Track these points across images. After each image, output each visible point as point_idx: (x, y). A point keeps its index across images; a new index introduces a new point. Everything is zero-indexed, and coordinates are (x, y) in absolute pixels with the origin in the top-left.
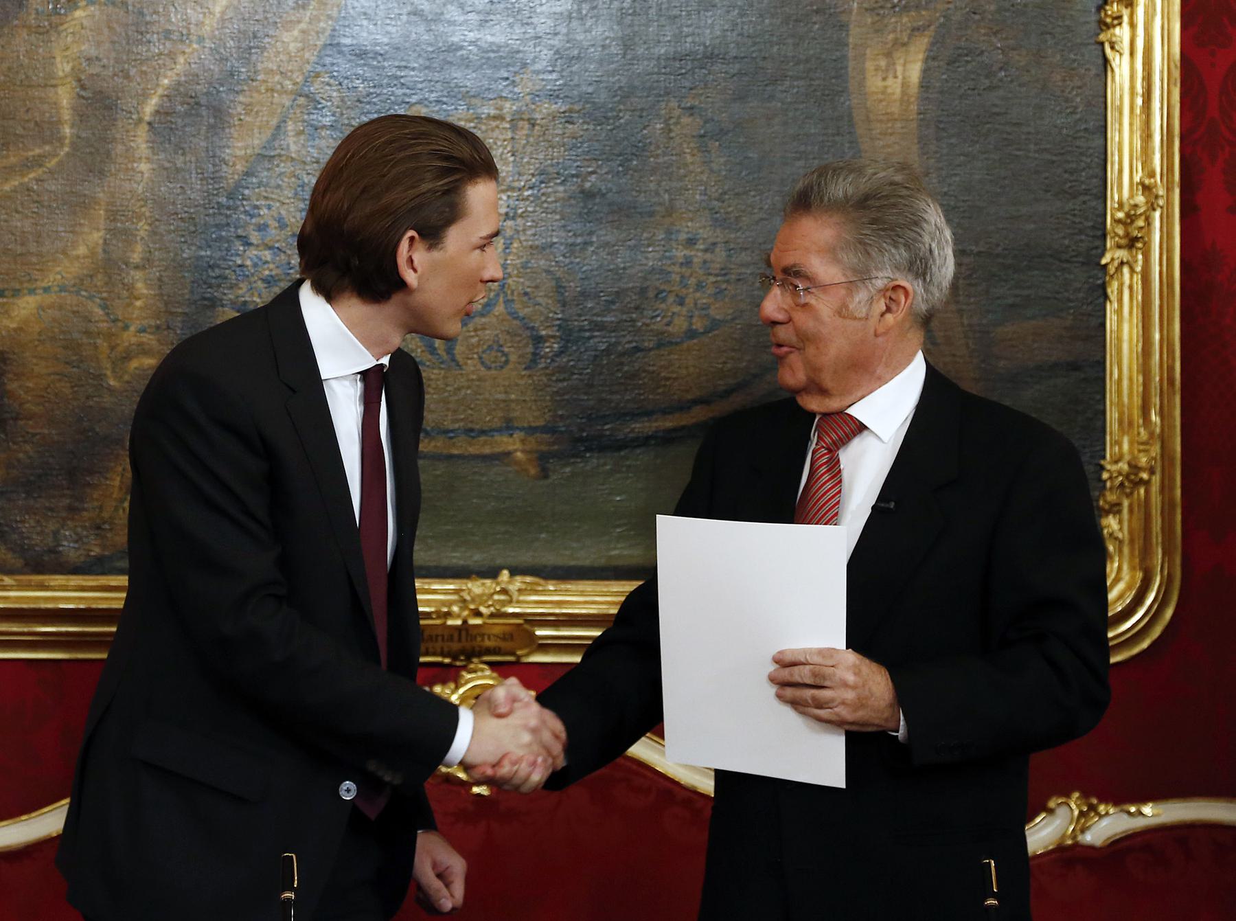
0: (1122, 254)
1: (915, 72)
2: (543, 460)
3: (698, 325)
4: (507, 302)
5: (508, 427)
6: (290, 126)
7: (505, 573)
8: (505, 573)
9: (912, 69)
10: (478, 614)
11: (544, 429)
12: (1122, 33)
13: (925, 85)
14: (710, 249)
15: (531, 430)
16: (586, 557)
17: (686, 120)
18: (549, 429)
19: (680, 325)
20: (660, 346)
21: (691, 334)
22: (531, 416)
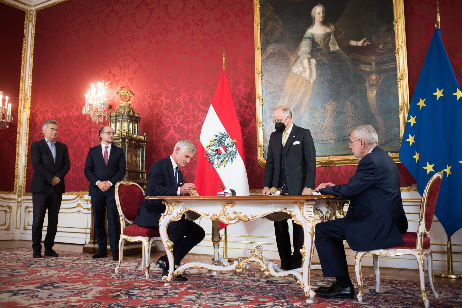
0: (401, 112)
1: (375, 94)
2: (335, 142)
3: (351, 126)
4: (330, 125)
5: (331, 139)
6: (306, 108)
7: (331, 156)
8: (331, 156)
9: (375, 93)
10: (327, 160)
11: (335, 139)
12: (399, 85)
13: (376, 95)
14: (352, 117)
15: (333, 139)
16: (340, 153)
17: (349, 102)
18: (335, 139)
19: (349, 126)
20: (347, 128)
21: (351, 127)
22: (333, 138)
